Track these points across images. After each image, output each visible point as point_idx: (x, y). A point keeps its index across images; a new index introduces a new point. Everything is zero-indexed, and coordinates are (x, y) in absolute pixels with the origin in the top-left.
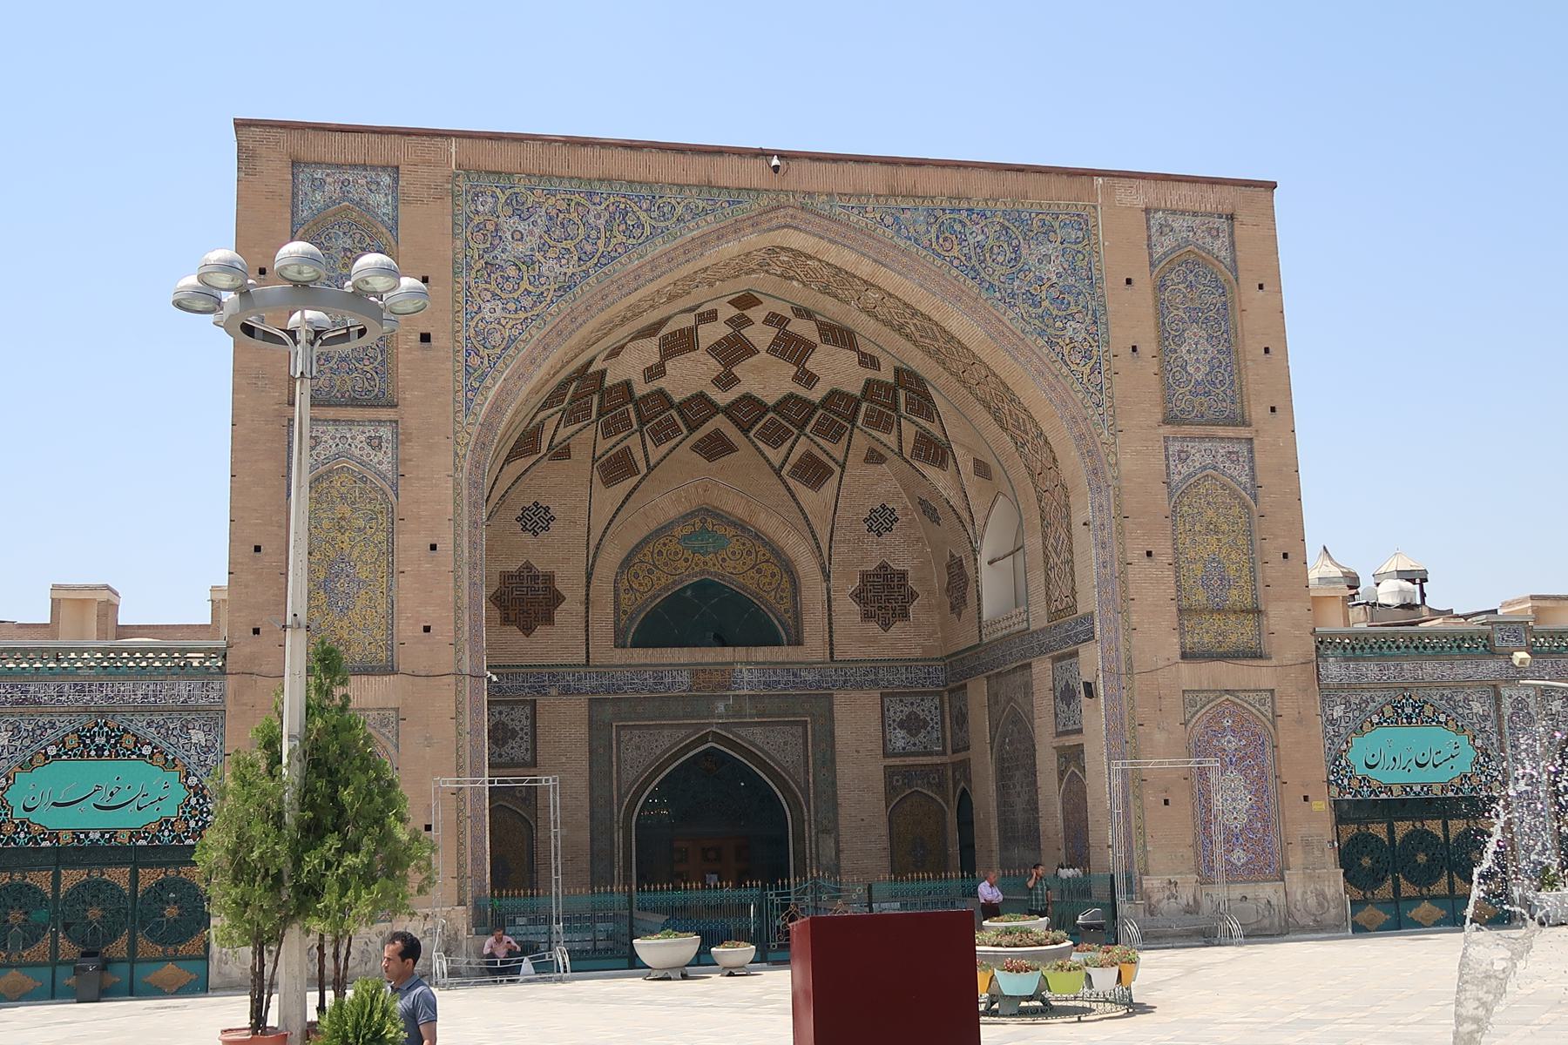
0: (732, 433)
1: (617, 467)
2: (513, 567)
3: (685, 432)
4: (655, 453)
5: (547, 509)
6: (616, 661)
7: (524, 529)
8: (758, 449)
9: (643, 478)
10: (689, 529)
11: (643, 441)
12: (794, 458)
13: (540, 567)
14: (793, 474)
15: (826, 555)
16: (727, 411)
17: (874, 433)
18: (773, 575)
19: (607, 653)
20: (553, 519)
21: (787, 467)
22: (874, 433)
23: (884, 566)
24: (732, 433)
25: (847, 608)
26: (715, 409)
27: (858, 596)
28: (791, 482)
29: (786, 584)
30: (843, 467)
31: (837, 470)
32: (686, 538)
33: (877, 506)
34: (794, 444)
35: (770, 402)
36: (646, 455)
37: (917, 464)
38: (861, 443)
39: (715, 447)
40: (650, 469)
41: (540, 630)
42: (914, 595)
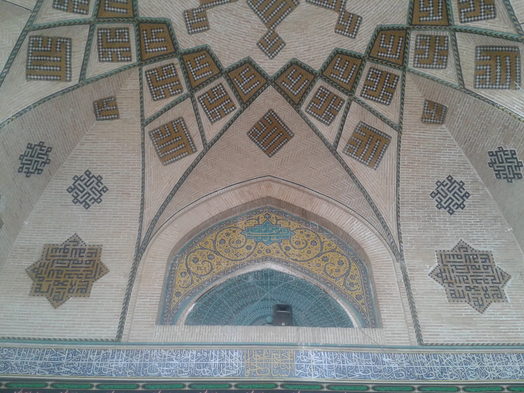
0: (285, 112)
1: (171, 140)
2: (59, 239)
3: (238, 107)
4: (212, 130)
5: (99, 179)
6: (155, 339)
7: (76, 201)
8: (310, 125)
9: (201, 157)
10: (252, 223)
11: (196, 110)
12: (348, 132)
13: (88, 240)
14: (349, 151)
15: (395, 234)
16: (275, 81)
17: (429, 72)
18: (341, 263)
19: (143, 327)
20: (105, 190)
21: (342, 143)
22: (429, 72)
23: (462, 247)
24: (285, 112)
25: (430, 291)
26: (266, 81)
27: (440, 275)
28: (349, 161)
29: (355, 270)
30: (399, 129)
31: (393, 134)
32: (248, 229)
33: (443, 178)
34: (345, 117)
35: (317, 65)
36: (202, 132)
37: (483, 93)
38: (414, 93)
39: (271, 135)
40: (208, 147)
41: (72, 303)
42: (504, 277)
